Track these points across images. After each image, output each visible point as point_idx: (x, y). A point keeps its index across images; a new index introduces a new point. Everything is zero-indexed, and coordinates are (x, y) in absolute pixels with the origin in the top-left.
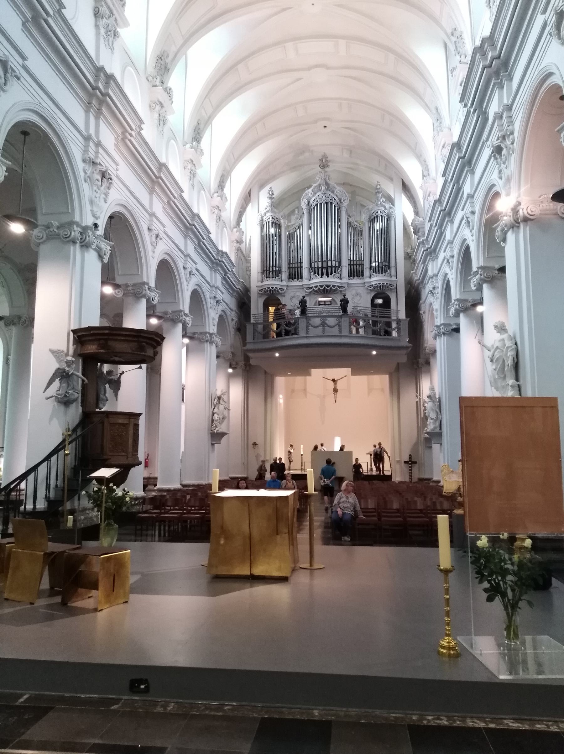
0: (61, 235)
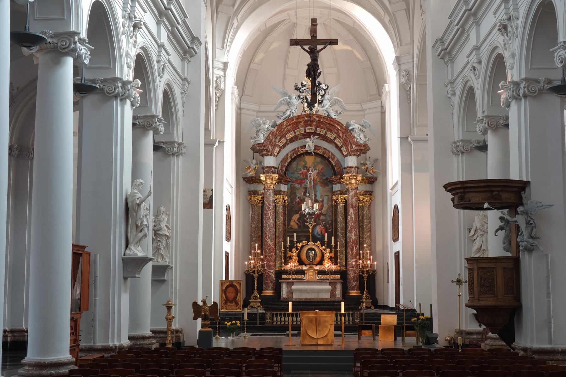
0: (105, 90)
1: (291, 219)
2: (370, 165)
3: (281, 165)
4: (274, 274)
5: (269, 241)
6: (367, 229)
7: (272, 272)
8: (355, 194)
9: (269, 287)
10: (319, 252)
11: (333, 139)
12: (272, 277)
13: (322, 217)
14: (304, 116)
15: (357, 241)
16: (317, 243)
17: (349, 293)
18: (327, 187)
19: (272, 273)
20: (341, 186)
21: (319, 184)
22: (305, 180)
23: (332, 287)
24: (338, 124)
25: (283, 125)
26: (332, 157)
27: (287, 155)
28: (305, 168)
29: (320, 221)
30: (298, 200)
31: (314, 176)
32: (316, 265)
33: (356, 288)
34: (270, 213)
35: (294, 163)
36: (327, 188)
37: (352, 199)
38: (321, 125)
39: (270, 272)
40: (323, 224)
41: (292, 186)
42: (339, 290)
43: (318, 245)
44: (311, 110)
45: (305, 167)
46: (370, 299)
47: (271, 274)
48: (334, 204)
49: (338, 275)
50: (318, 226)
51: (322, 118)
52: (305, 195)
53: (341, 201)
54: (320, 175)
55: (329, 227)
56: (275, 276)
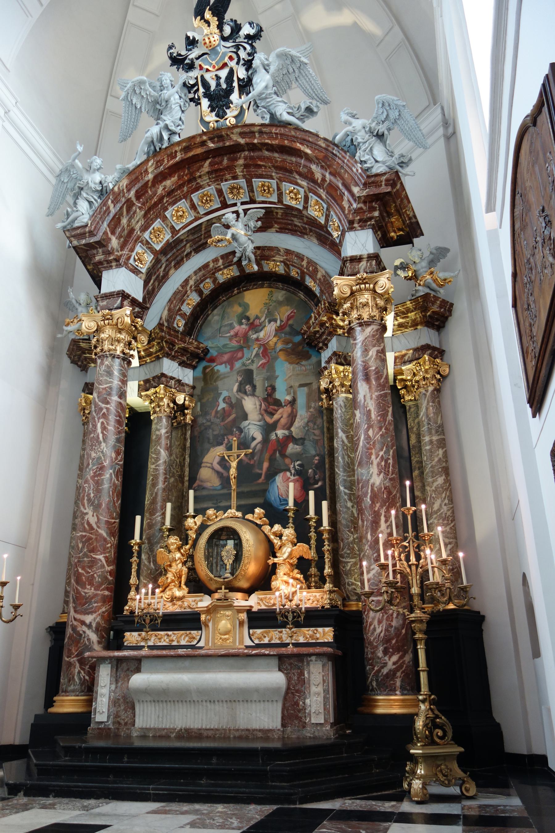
1: (202, 463)
2: (424, 264)
3: (169, 310)
4: (97, 630)
5: (87, 514)
6: (434, 463)
7: (88, 622)
8: (373, 336)
9: (71, 680)
10: (251, 542)
11: (304, 207)
12: (89, 640)
13: (292, 448)
14: (205, 138)
15: (390, 493)
16: (253, 513)
17: (373, 703)
18: (304, 363)
19: (89, 626)
20: (339, 342)
21: (282, 357)
22: (243, 351)
23: (289, 680)
24: (304, 141)
25: (146, 171)
26: (311, 269)
27: (186, 281)
28: (244, 321)
29: (287, 461)
30: (222, 405)
31: (269, 336)
32: (249, 592)
33: (398, 683)
34: (102, 423)
35: (215, 312)
36: (307, 365)
37: (366, 351)
38: (259, 163)
39: (83, 623)
40: (294, 467)
41: (208, 370)
42: (320, 689)
43: (258, 522)
44: (221, 115)
45: (243, 317)
46: (453, 739)
47: (84, 628)
48: (325, 405)
49: (327, 629)
50: (281, 474)
51: (257, 135)
52: (241, 390)
53: (342, 385)
54: (285, 334)
55: (315, 473)
56: (101, 637)
